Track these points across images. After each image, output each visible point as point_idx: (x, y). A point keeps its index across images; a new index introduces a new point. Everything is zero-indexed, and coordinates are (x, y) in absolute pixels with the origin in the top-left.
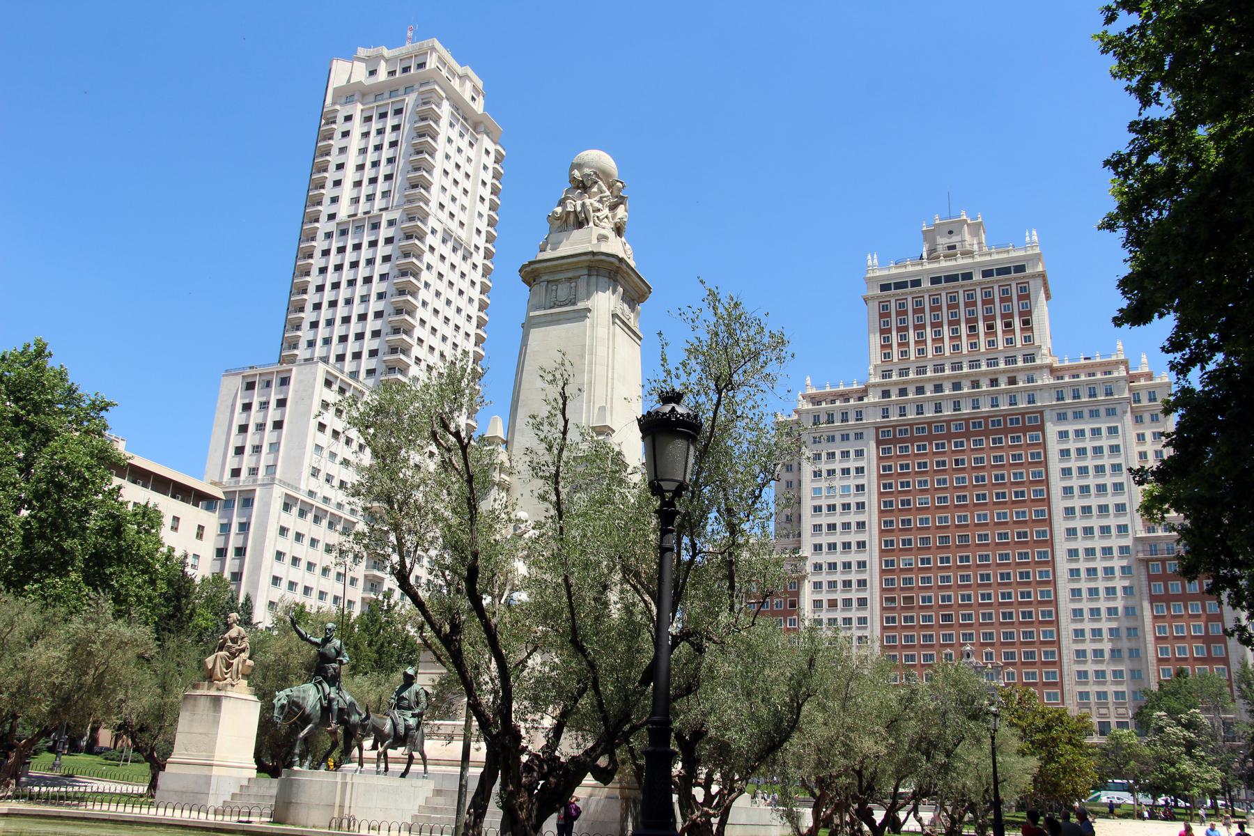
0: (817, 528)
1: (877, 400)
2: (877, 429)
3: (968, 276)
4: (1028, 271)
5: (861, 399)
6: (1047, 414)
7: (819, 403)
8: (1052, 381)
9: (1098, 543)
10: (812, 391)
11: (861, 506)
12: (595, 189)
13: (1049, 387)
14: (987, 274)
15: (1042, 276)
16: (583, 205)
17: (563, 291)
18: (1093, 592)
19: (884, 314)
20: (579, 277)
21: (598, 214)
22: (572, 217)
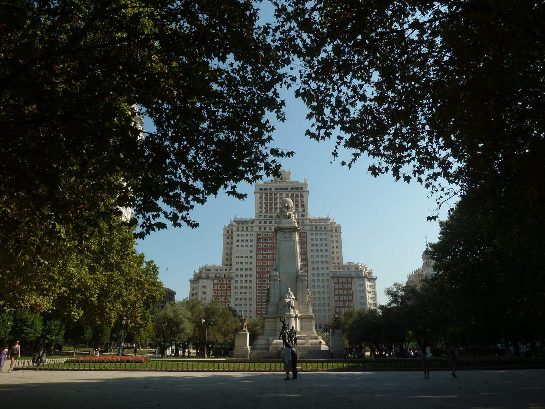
0: (237, 263)
1: (257, 224)
2: (257, 233)
3: (286, 189)
4: (304, 189)
5: (252, 223)
6: (308, 233)
7: (239, 224)
8: (309, 223)
9: (321, 272)
11: (251, 257)
13: (309, 225)
14: (292, 189)
15: (308, 191)
16: (290, 213)
17: (287, 235)
18: (319, 286)
19: (260, 198)
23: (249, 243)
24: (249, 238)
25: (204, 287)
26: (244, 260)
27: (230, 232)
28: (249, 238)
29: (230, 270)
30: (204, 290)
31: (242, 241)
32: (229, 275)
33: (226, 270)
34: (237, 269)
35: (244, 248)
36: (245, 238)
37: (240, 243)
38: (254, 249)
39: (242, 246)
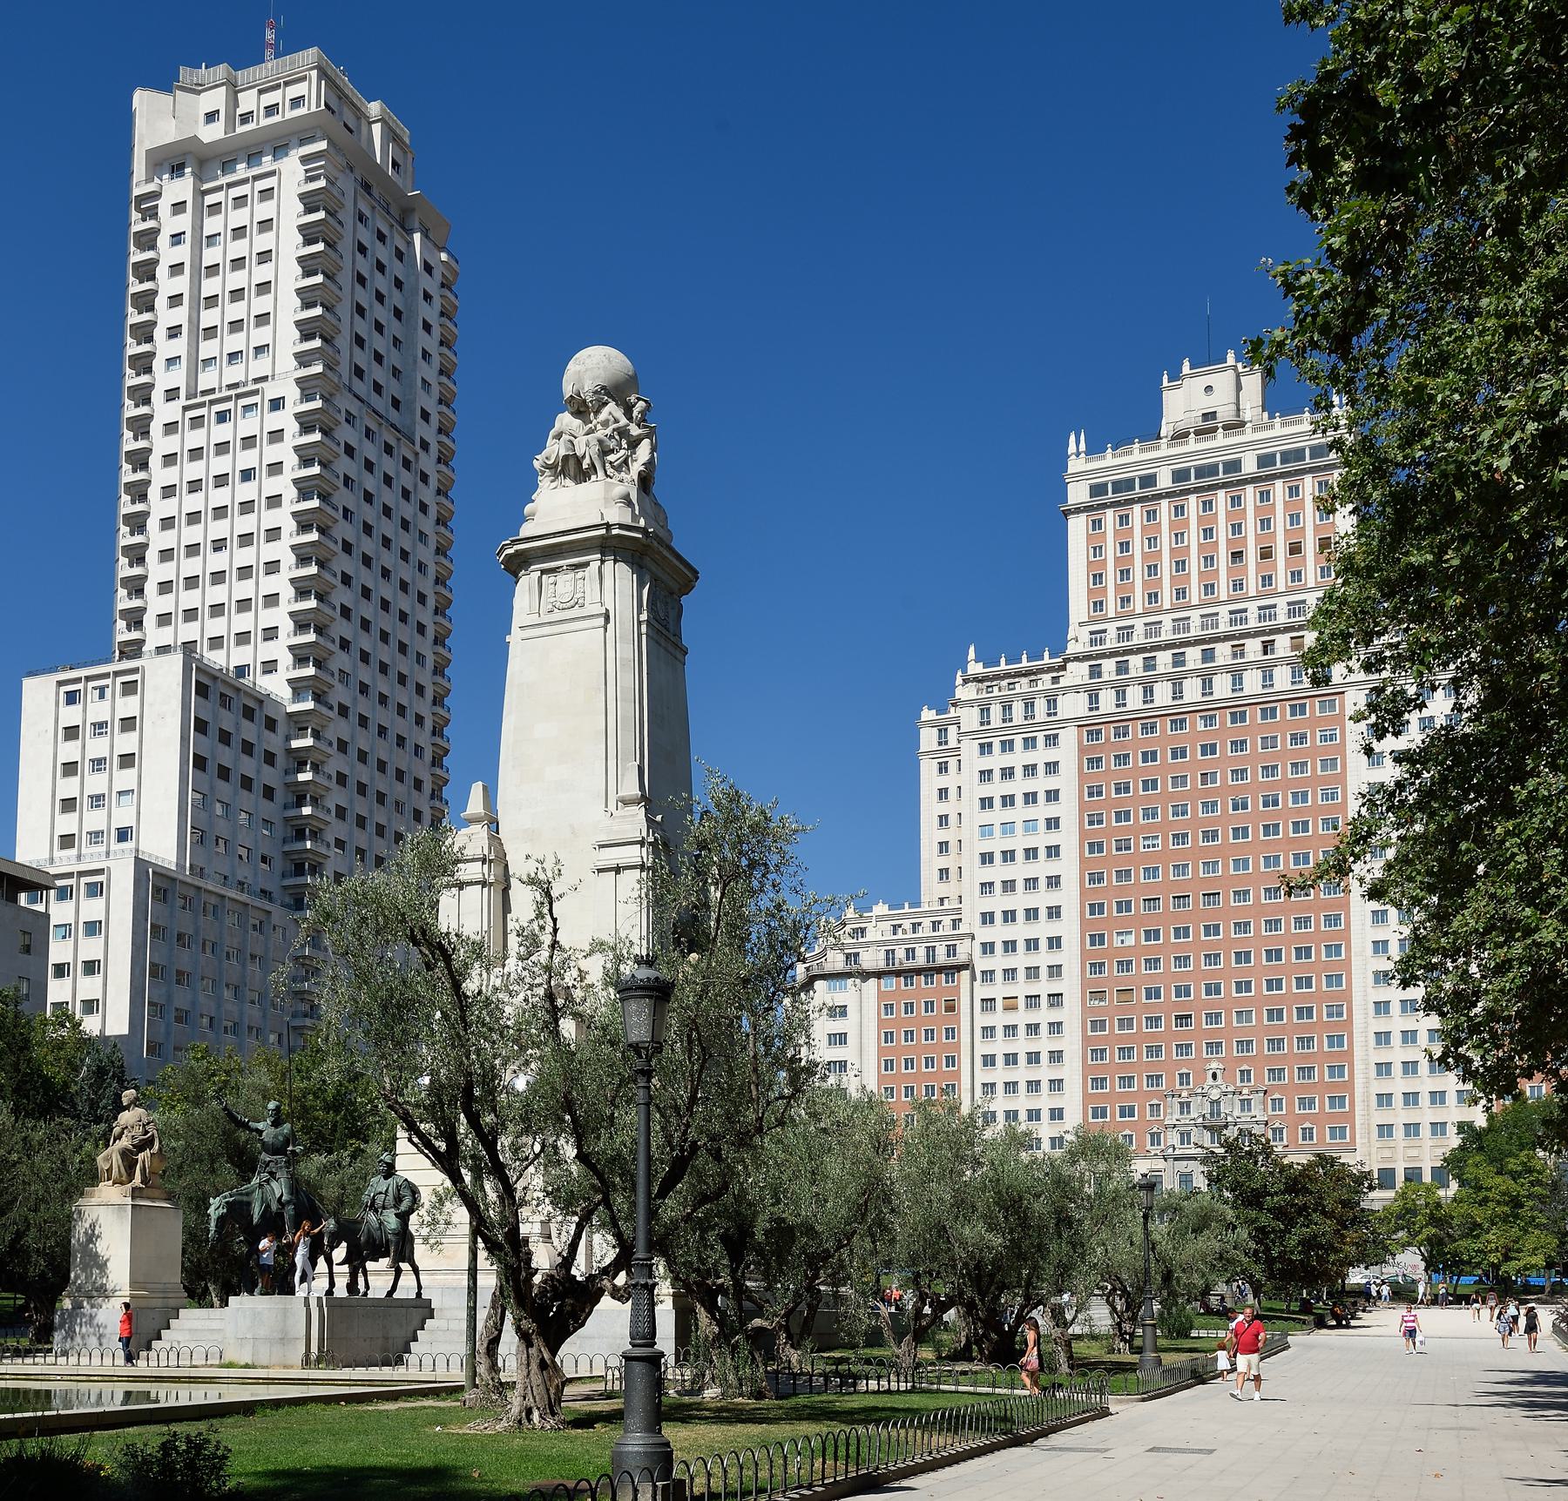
0: (987, 887)
10: (975, 668)
12: (603, 415)
17: (564, 584)
20: (586, 564)
21: (612, 458)
22: (572, 462)
23: (1041, 784)
24: (1041, 756)
25: (839, 1011)
26: (1019, 871)
27: (952, 730)
28: (1041, 756)
29: (956, 923)
30: (837, 1026)
31: (1008, 773)
32: (951, 951)
33: (935, 925)
34: (987, 918)
35: (1019, 813)
36: (1018, 758)
37: (997, 789)
38: (1067, 809)
39: (1008, 801)
